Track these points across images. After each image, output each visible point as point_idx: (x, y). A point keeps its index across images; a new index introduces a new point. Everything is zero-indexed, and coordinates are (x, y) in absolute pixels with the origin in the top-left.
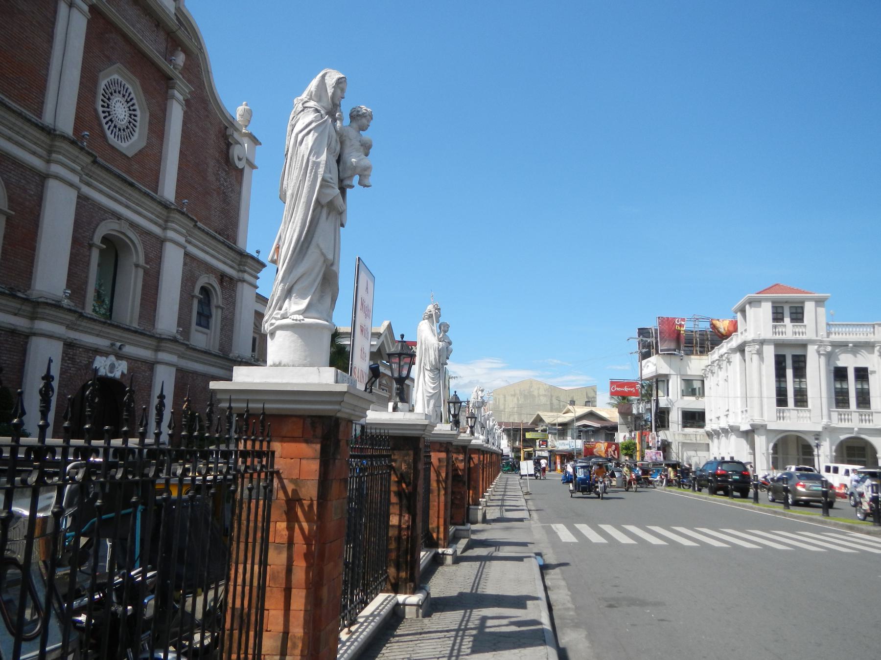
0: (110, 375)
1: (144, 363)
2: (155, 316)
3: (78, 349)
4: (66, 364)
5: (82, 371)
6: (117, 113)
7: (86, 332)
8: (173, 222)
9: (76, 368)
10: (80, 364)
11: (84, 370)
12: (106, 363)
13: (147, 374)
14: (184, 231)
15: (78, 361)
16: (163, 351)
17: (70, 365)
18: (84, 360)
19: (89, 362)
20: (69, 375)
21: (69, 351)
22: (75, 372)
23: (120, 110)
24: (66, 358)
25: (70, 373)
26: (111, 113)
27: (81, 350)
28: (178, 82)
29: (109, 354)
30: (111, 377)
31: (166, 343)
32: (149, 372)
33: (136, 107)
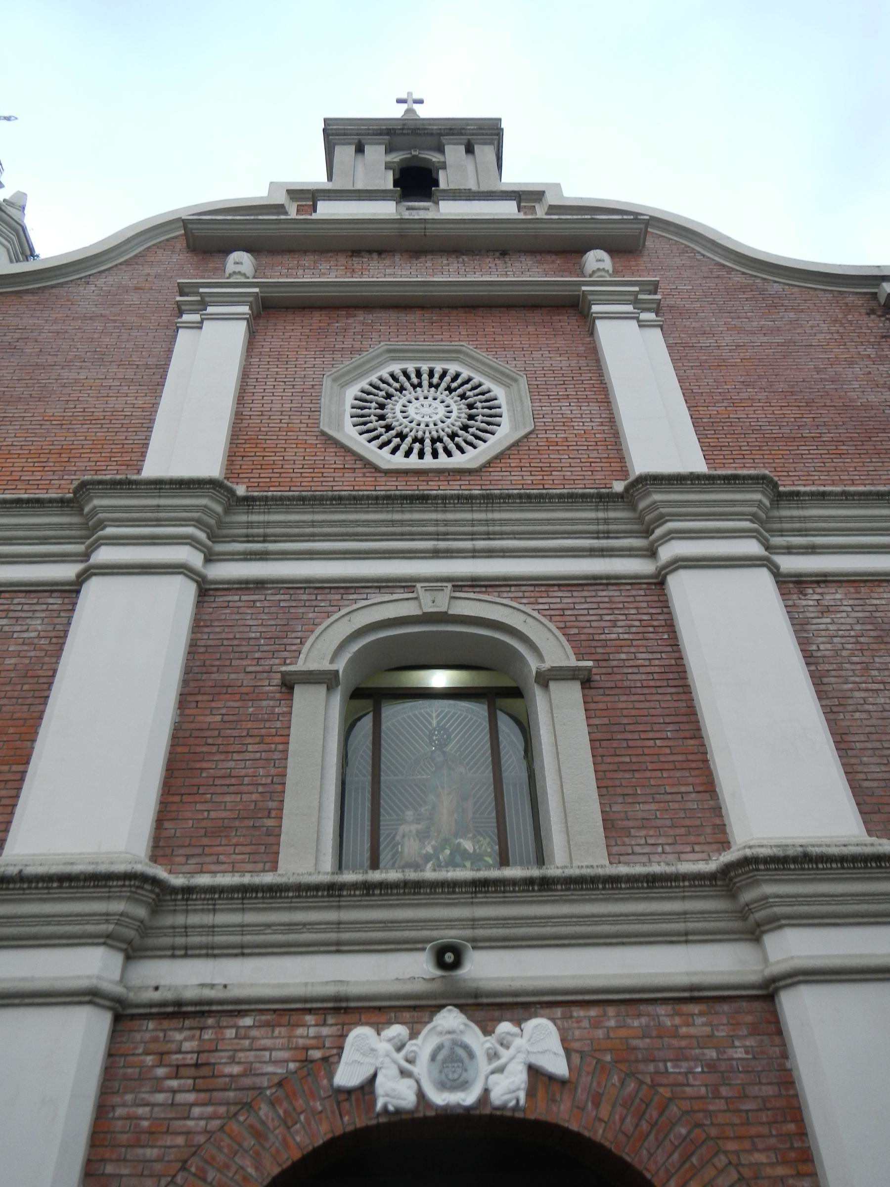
0: (440, 1098)
1: (695, 1008)
2: (717, 810)
3: (224, 1021)
4: (160, 1097)
5: (264, 1110)
6: (427, 419)
7: (242, 951)
8: (661, 519)
9: (228, 1104)
10: (247, 1082)
11: (272, 1103)
12: (411, 1046)
13: (739, 1053)
14: (747, 524)
15: (236, 1069)
16: (776, 923)
17: (191, 1097)
18: (271, 1062)
19: (307, 1061)
20: (180, 1140)
21: (178, 1036)
22: (215, 1124)
23: (426, 410)
24: (161, 1072)
25: (188, 1133)
26: (420, 434)
27: (248, 1021)
28: (584, 288)
29: (441, 1007)
30: (468, 1109)
31: (756, 883)
32: (750, 1042)
33: (411, 367)
